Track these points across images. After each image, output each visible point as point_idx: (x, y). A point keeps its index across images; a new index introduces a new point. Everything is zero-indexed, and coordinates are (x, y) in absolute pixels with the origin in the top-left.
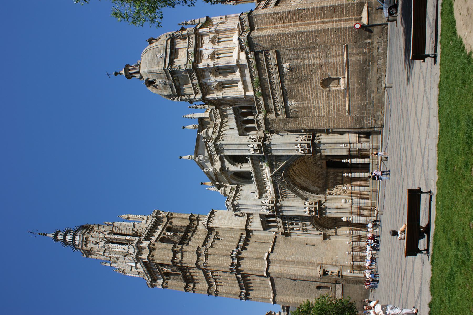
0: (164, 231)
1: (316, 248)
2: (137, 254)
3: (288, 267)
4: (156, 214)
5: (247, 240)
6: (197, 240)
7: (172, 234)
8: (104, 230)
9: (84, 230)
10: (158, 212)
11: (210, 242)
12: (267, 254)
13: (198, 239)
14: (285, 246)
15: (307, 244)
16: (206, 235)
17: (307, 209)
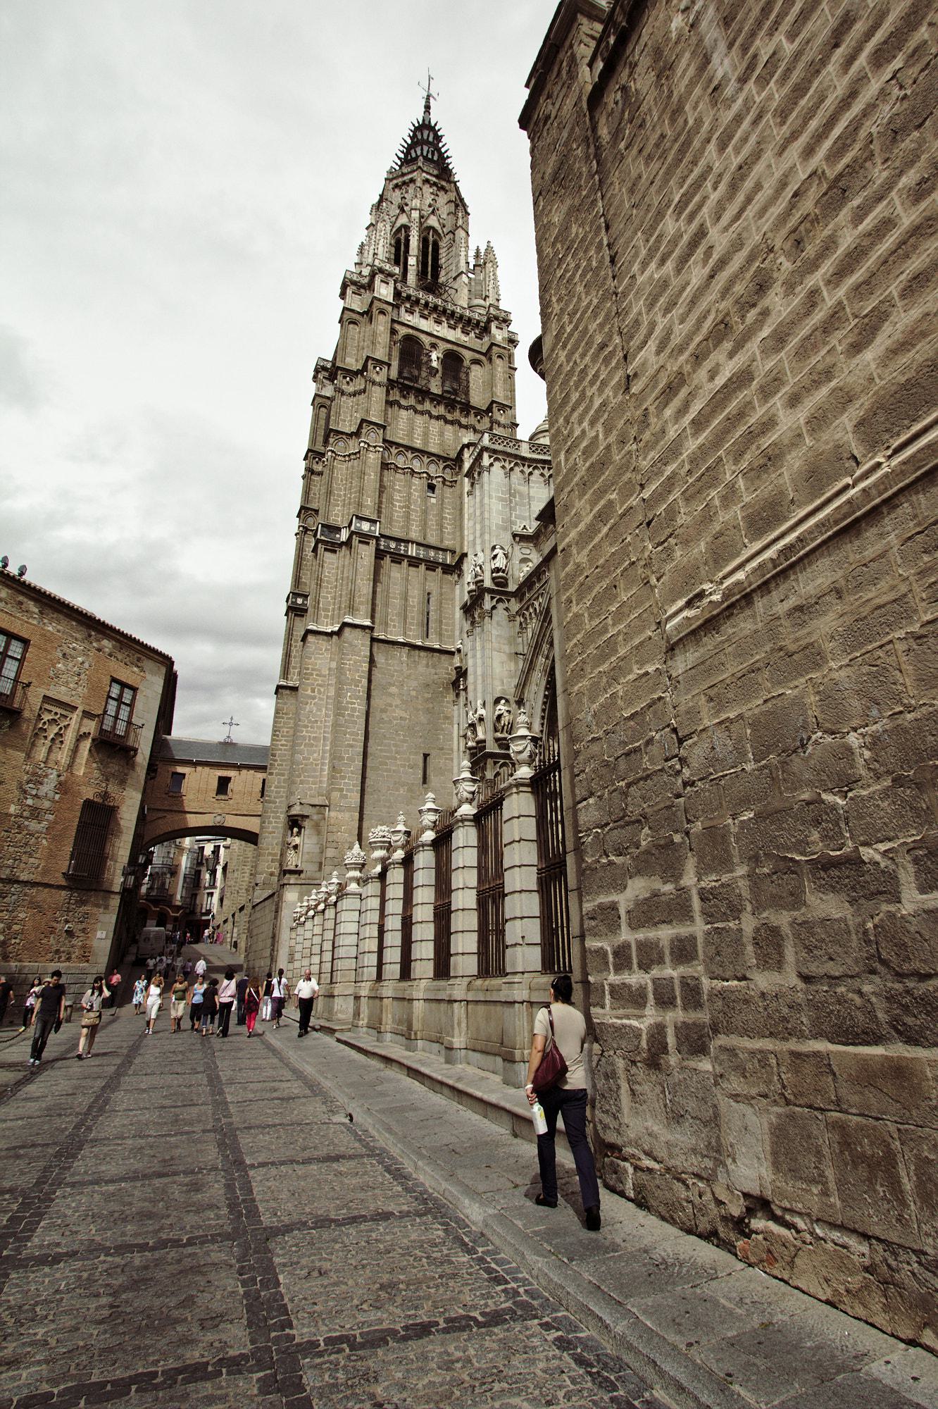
0: (443, 346)
1: (410, 790)
2: (354, 283)
3: (328, 697)
4: (496, 318)
5: (432, 566)
6: (419, 431)
7: (435, 364)
8: (444, 216)
9: (436, 172)
10: (506, 321)
11: (416, 465)
12: (367, 623)
13: (426, 435)
14: (414, 684)
15: (426, 756)
16: (442, 454)
17: (481, 711)
